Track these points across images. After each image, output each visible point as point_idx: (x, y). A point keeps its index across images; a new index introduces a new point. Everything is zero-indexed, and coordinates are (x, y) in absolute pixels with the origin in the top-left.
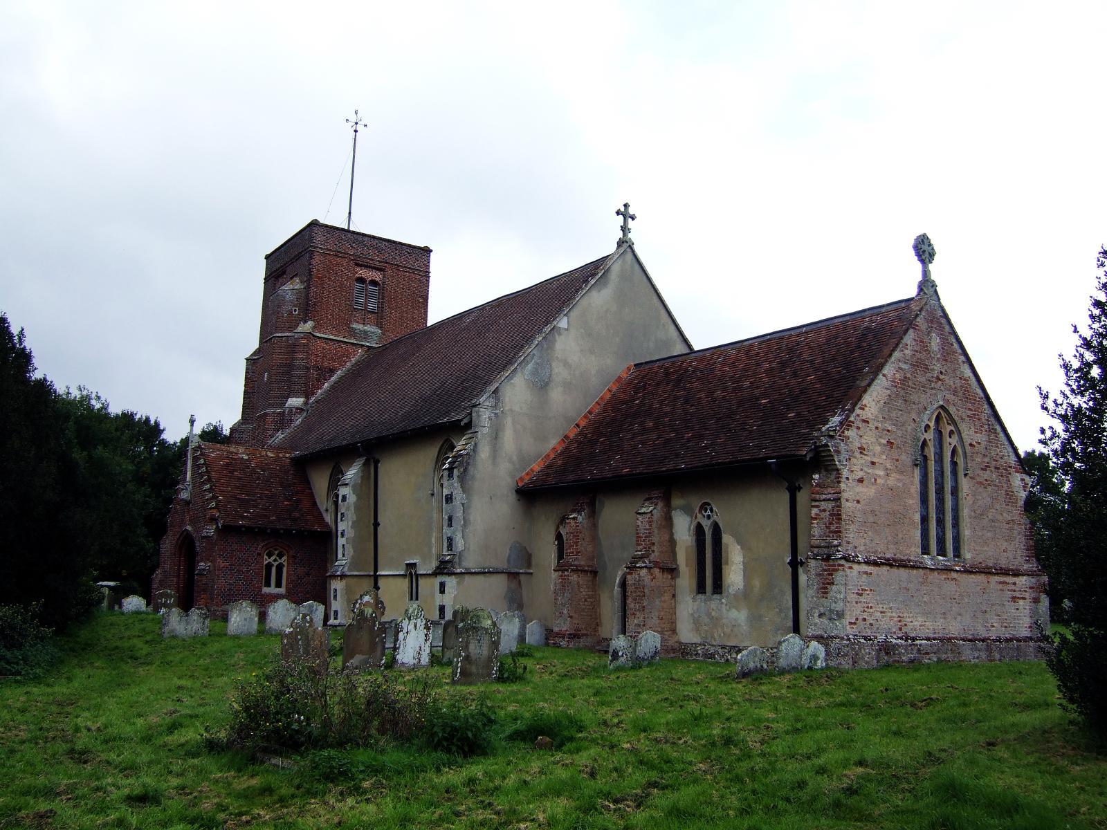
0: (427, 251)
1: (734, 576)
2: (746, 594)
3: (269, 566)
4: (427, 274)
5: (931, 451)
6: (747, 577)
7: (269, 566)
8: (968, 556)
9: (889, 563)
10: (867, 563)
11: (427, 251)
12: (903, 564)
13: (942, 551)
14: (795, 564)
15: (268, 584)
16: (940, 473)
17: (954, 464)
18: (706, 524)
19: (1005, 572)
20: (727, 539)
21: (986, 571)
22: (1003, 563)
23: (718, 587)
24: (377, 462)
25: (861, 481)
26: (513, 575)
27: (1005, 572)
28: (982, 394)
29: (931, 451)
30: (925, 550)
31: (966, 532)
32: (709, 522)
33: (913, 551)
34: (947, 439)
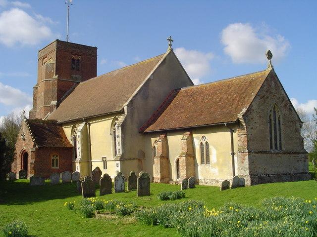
0: (96, 48)
1: (213, 157)
2: (218, 163)
3: (53, 160)
4: (96, 56)
5: (272, 118)
6: (218, 158)
7: (53, 160)
8: (283, 148)
9: (261, 152)
10: (255, 153)
11: (96, 48)
12: (265, 152)
13: (276, 148)
14: (233, 154)
15: (53, 166)
16: (275, 124)
17: (279, 121)
18: (204, 143)
19: (295, 153)
20: (211, 147)
21: (289, 153)
22: (295, 150)
23: (208, 161)
24: (89, 124)
25: (252, 128)
26: (139, 160)
27: (295, 153)
28: (287, 99)
29: (272, 118)
30: (271, 148)
31: (283, 142)
32: (205, 142)
33: (268, 149)
34: (277, 113)
